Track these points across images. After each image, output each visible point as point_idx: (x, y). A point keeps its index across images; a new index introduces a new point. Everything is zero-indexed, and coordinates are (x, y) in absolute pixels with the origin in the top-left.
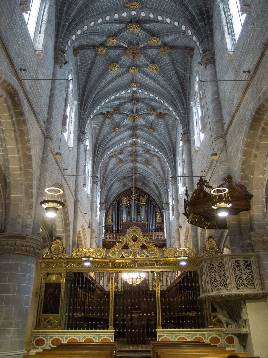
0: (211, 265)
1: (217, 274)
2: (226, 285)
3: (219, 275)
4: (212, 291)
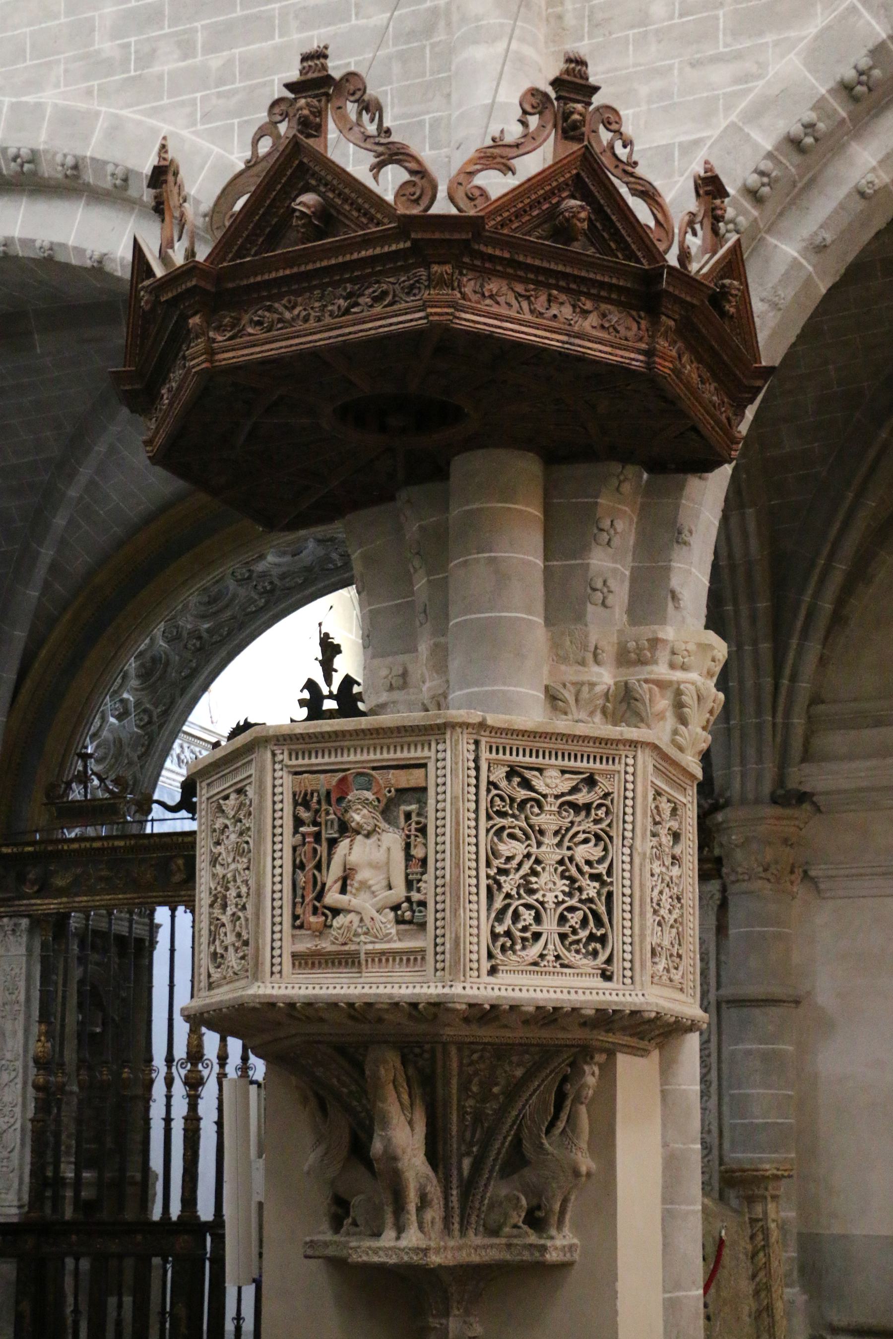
0: (517, 780)
1: (550, 852)
2: (603, 940)
3: (561, 862)
4: (493, 971)
